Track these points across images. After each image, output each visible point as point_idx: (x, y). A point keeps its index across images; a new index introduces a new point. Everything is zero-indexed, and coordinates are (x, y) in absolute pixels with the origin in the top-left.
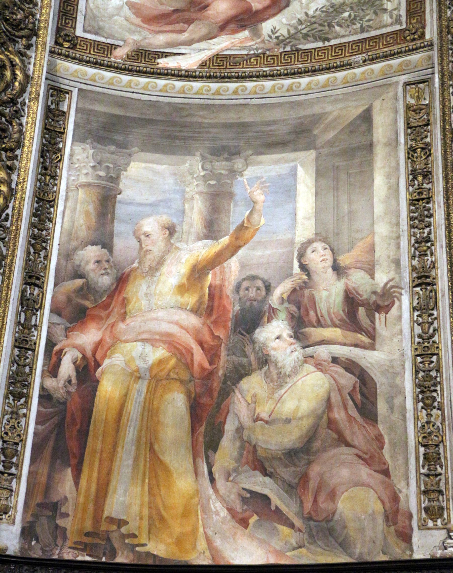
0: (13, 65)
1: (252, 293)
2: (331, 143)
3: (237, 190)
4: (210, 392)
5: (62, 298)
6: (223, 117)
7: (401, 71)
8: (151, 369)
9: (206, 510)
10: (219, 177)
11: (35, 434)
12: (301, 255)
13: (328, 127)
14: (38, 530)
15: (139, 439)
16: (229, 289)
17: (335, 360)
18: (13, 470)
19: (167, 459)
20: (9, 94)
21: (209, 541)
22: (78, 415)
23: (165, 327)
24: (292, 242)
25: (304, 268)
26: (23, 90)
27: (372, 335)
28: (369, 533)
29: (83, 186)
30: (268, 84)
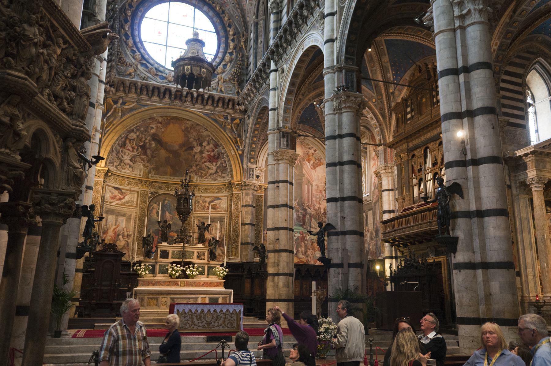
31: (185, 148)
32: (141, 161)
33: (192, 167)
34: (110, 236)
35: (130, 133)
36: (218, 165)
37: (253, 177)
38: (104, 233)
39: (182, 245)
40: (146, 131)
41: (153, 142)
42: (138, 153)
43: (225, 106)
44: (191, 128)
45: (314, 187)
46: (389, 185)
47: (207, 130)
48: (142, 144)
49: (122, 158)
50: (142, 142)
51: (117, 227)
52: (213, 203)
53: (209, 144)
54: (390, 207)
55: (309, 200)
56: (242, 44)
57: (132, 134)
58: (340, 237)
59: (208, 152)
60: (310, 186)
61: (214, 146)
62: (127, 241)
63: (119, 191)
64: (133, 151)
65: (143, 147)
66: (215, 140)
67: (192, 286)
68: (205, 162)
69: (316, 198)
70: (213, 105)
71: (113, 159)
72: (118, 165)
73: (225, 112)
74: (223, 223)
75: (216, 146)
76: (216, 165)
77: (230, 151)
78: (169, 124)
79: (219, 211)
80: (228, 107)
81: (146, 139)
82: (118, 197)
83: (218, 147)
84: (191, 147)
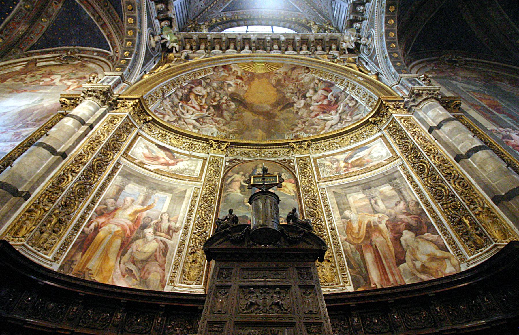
0: (111, 155)
1: (147, 221)
2: (176, 194)
3: (152, 197)
4: (128, 241)
5: (99, 209)
6: (155, 181)
7: (195, 185)
8: (115, 232)
9: (115, 271)
10: (149, 193)
11: (76, 241)
12: (162, 215)
13: (177, 190)
14: (65, 267)
15: (105, 248)
16: (142, 218)
17: (161, 241)
18: (65, 249)
19: (110, 255)
20: (107, 160)
21: (113, 279)
22: (90, 239)
23: (122, 223)
24: (160, 212)
25: (161, 218)
26: (110, 161)
27: (171, 237)
28: (155, 284)
29: (116, 185)
30: (167, 178)
31: (281, 106)
32: (214, 124)
33: (296, 126)
34: (122, 227)
35: (196, 86)
38: (101, 214)
40: (221, 89)
41: (232, 103)
42: (209, 114)
44: (285, 79)
48: (215, 104)
49: (182, 116)
50: (215, 102)
51: (146, 210)
52: (354, 159)
57: (199, 88)
59: (318, 102)
62: (164, 243)
63: (167, 153)
64: (201, 110)
65: (218, 108)
66: (324, 80)
71: (164, 109)
72: (174, 122)
74: (398, 181)
75: (328, 87)
76: (337, 112)
78: (253, 79)
80: (331, 49)
81: (221, 99)
82: (162, 161)
83: (332, 88)
84: (289, 104)
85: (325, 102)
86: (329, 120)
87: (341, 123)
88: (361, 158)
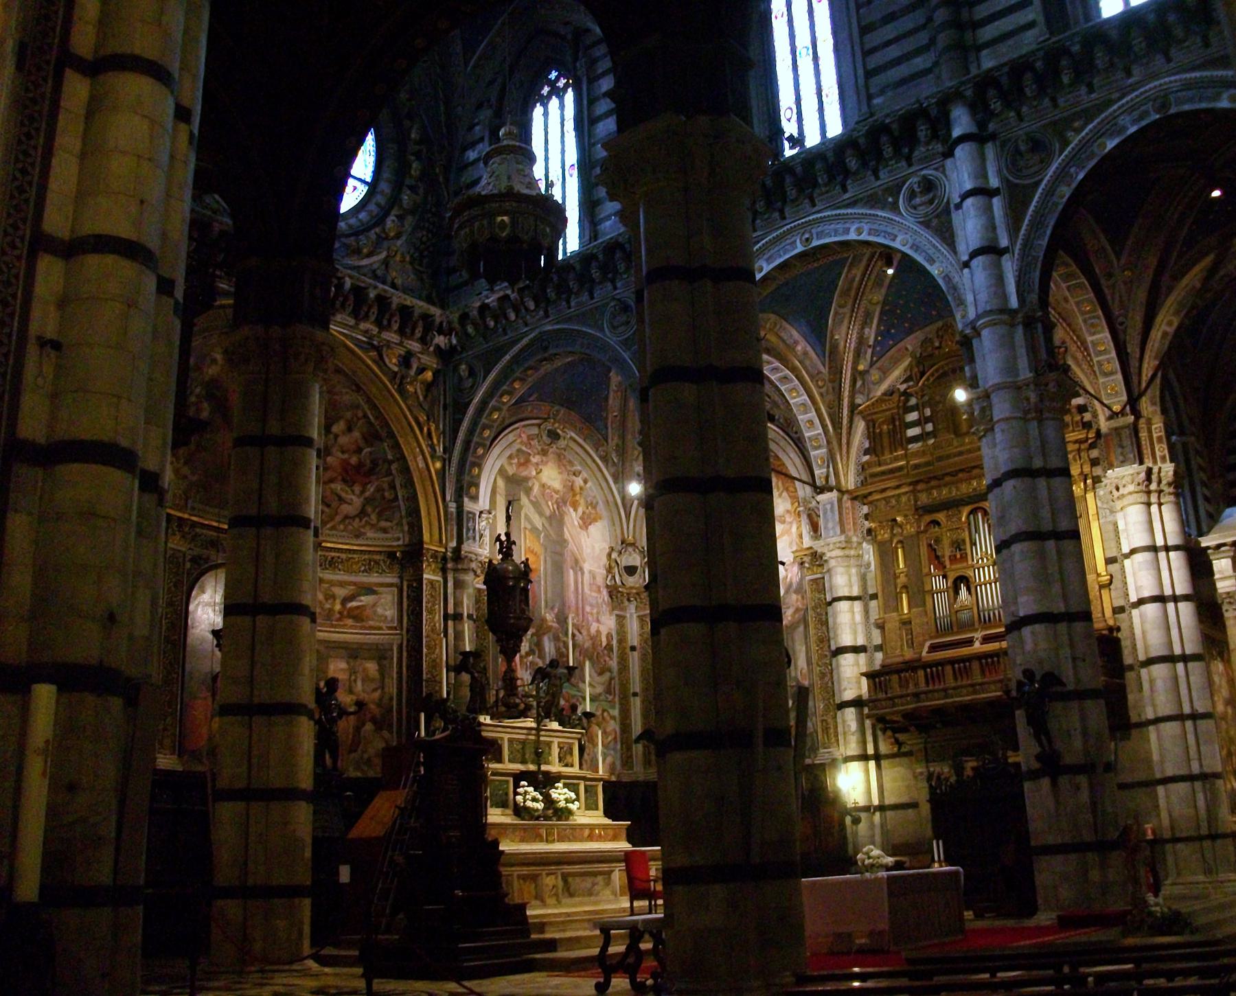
36: (367, 494)
37: (474, 538)
39: (530, 723)
43: (408, 331)
45: (587, 576)
46: (851, 586)
47: (358, 389)
52: (354, 604)
53: (350, 429)
54: (855, 639)
55: (577, 609)
56: (437, 170)
58: (1075, 704)
59: (343, 452)
60: (579, 573)
61: (364, 438)
67: (570, 840)
68: (332, 481)
69: (591, 605)
70: (378, 323)
73: (401, 344)
76: (363, 492)
77: (415, 458)
79: (371, 628)
80: (411, 336)
85: (354, 460)
86: (346, 502)
87: (361, 520)
88: (363, 606)
